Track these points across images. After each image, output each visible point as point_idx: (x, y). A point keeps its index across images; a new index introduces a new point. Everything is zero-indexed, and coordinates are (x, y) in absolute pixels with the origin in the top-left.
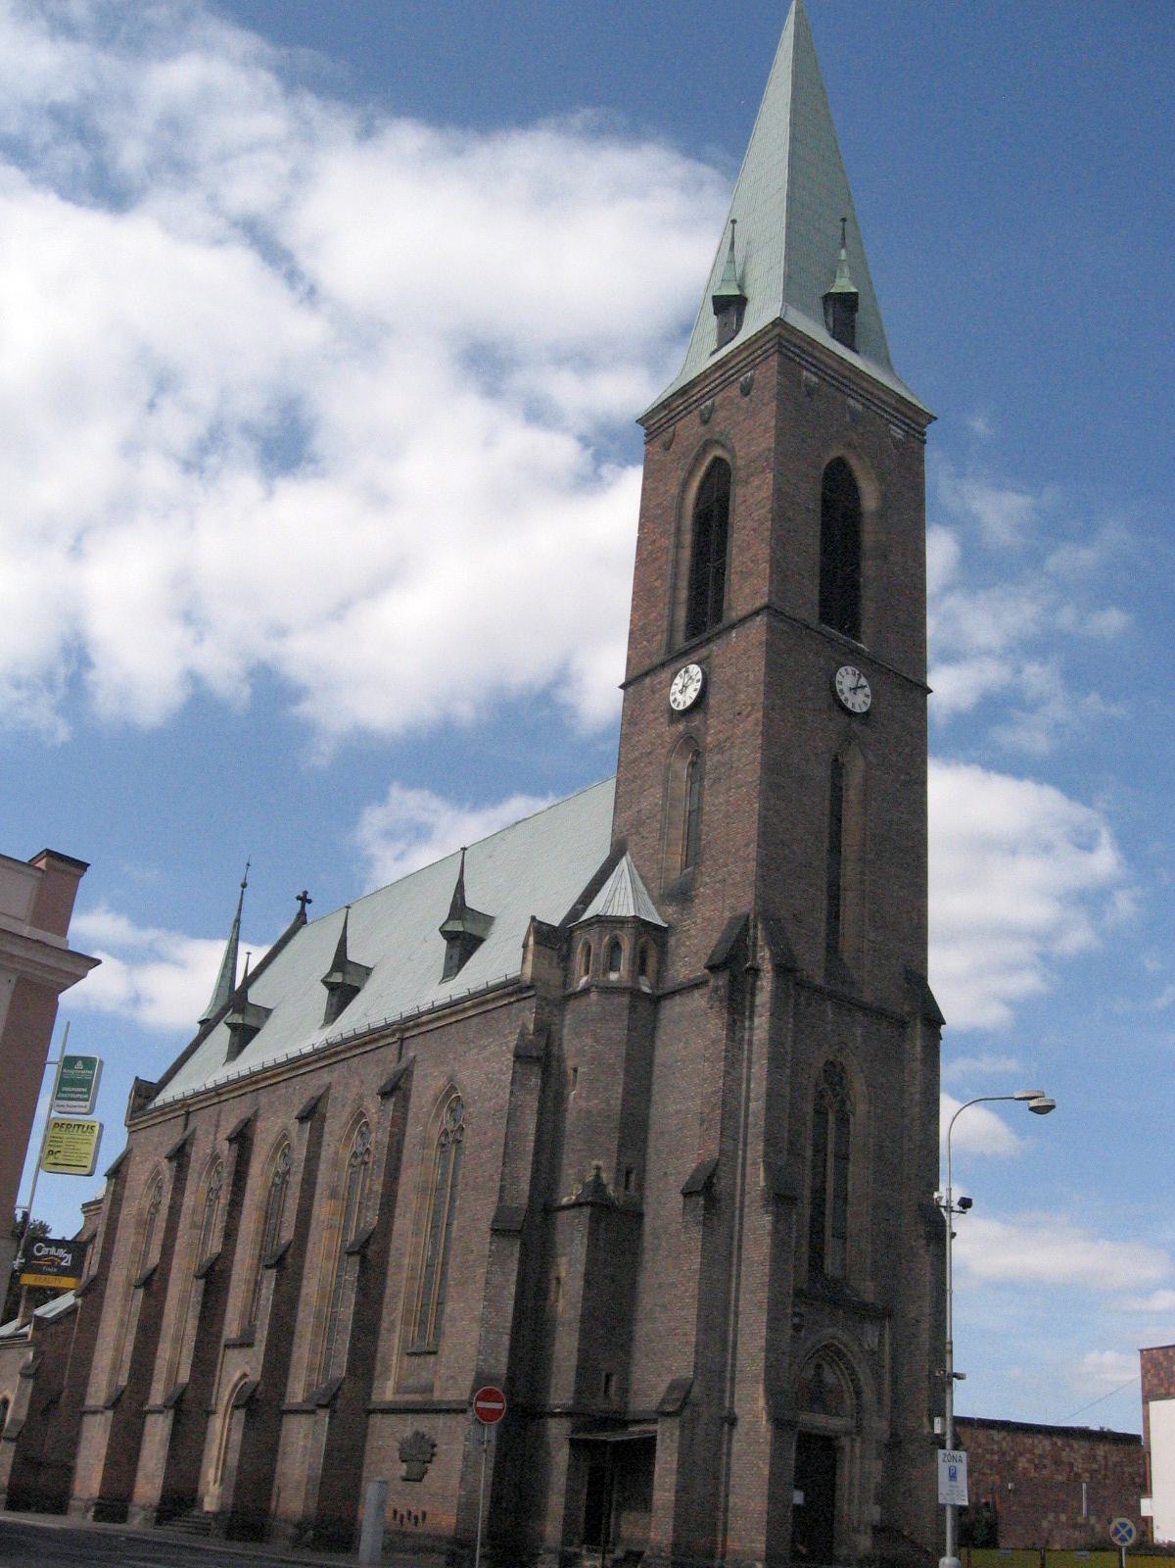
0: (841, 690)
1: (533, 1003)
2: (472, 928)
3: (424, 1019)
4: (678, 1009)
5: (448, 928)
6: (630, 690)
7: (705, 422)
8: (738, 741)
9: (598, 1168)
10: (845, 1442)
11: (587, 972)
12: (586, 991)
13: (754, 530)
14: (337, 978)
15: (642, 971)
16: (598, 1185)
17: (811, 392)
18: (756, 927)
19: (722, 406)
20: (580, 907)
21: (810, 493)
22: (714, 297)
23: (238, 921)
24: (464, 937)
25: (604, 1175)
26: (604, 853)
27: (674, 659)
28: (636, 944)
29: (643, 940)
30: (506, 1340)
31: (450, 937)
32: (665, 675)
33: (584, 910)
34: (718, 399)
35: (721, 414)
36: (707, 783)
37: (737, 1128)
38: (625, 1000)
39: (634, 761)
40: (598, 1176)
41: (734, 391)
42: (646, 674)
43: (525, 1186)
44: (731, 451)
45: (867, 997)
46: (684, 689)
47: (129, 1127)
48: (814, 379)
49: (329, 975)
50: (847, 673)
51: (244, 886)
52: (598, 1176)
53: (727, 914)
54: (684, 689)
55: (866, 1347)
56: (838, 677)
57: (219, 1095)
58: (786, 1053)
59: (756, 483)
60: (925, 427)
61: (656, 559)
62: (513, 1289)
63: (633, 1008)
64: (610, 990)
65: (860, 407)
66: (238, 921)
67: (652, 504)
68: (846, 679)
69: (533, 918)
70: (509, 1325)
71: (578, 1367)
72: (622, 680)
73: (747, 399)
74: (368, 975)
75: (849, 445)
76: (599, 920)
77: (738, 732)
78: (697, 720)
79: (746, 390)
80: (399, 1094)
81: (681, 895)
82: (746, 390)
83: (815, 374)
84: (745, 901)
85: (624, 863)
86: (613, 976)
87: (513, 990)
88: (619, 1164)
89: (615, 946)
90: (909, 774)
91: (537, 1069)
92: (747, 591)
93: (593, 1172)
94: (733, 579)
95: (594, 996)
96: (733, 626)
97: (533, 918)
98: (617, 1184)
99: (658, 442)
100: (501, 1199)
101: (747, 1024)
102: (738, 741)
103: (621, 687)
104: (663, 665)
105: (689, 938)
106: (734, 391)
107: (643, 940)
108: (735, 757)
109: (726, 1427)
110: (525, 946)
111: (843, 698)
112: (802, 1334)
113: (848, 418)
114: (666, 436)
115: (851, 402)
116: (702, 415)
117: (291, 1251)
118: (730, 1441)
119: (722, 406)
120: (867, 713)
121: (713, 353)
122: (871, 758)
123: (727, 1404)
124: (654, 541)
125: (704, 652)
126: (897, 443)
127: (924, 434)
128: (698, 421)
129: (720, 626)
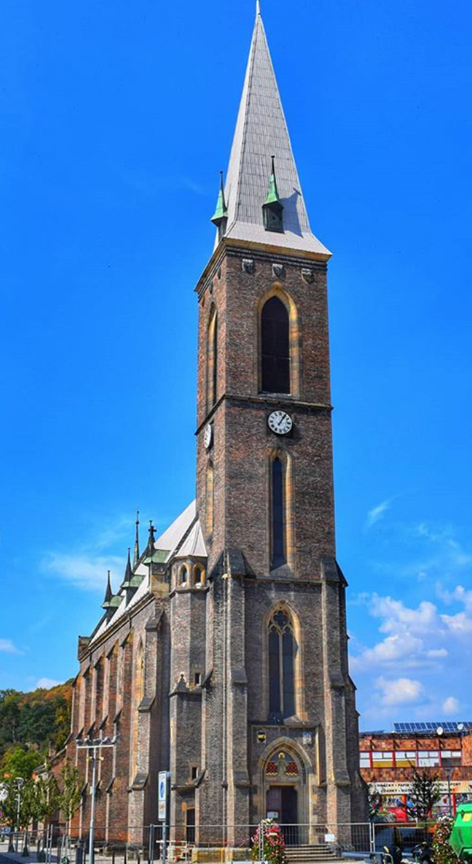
1: (154, 602)
9: (182, 676)
10: (297, 788)
16: (182, 683)
18: (226, 557)
21: (249, 326)
23: (137, 542)
25: (184, 678)
28: (192, 568)
29: (195, 566)
30: (147, 758)
37: (222, 653)
38: (189, 595)
40: (182, 679)
43: (154, 688)
47: (80, 660)
48: (250, 261)
49: (123, 584)
51: (137, 523)
52: (182, 679)
55: (304, 743)
57: (96, 645)
60: (325, 262)
62: (149, 736)
63: (192, 599)
64: (182, 592)
66: (137, 542)
70: (148, 751)
71: (177, 767)
80: (128, 645)
84: (223, 547)
85: (198, 522)
86: (184, 584)
87: (150, 596)
88: (190, 672)
91: (156, 633)
93: (181, 677)
95: (177, 595)
98: (191, 680)
100: (145, 695)
101: (225, 603)
109: (224, 789)
112: (265, 742)
113: (274, 275)
117: (108, 720)
118: (226, 795)
123: (224, 779)
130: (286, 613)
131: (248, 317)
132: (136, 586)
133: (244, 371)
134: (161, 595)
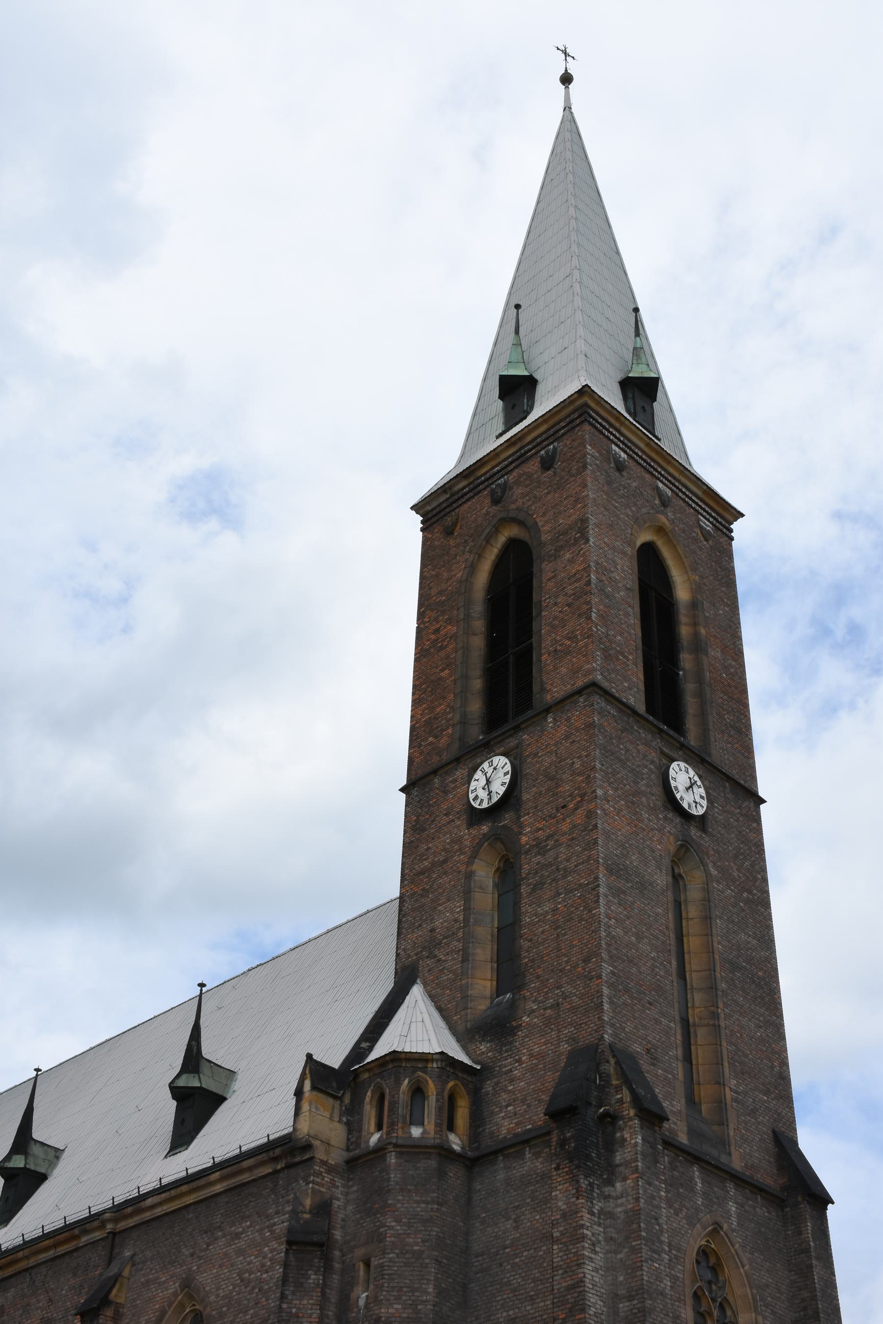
0: (676, 788)
2: (208, 1082)
3: (149, 1202)
4: (501, 1176)
5: (181, 1083)
6: (415, 792)
7: (496, 501)
8: (564, 839)
11: (379, 1127)
12: (380, 1151)
13: (569, 605)
14: (18, 1162)
15: (451, 1128)
17: (620, 467)
19: (517, 483)
20: (364, 1045)
22: (503, 379)
24: (196, 1100)
26: (386, 985)
27: (471, 756)
29: (451, 1084)
31: (178, 1093)
32: (460, 773)
33: (371, 1049)
34: (511, 478)
35: (518, 491)
36: (524, 890)
39: (422, 872)
41: (533, 466)
42: (435, 772)
44: (531, 527)
45: (737, 1163)
46: (490, 780)
50: (681, 770)
53: (565, 1047)
54: (490, 780)
56: (672, 773)
58: (661, 1231)
59: (568, 556)
61: (442, 648)
64: (412, 1150)
65: (669, 493)
67: (434, 591)
68: (681, 775)
69: (309, 1056)
72: (403, 782)
73: (550, 472)
74: (58, 1158)
75: (660, 530)
76: (394, 1057)
77: (565, 827)
78: (507, 819)
79: (547, 464)
81: (492, 1029)
82: (547, 464)
83: (625, 452)
85: (417, 992)
86: (416, 1132)
87: (284, 1154)
89: (418, 1092)
90: (750, 893)
92: (564, 670)
94: (545, 658)
96: (548, 710)
97: (309, 1056)
99: (437, 529)
102: (564, 839)
103: (402, 790)
104: (457, 760)
105: (512, 1081)
106: (533, 466)
107: (451, 1084)
108: (562, 857)
110: (299, 1093)
111: (678, 796)
113: (657, 502)
114: (449, 520)
115: (660, 485)
116: (493, 492)
119: (517, 483)
120: (703, 816)
121: (501, 435)
122: (714, 872)
124: (437, 631)
125: (512, 742)
126: (706, 536)
127: (731, 531)
128: (488, 501)
129: (530, 713)
130: (718, 1258)
131: (624, 553)
132: (42, 1170)
133: (622, 654)
134: (328, 1152)
